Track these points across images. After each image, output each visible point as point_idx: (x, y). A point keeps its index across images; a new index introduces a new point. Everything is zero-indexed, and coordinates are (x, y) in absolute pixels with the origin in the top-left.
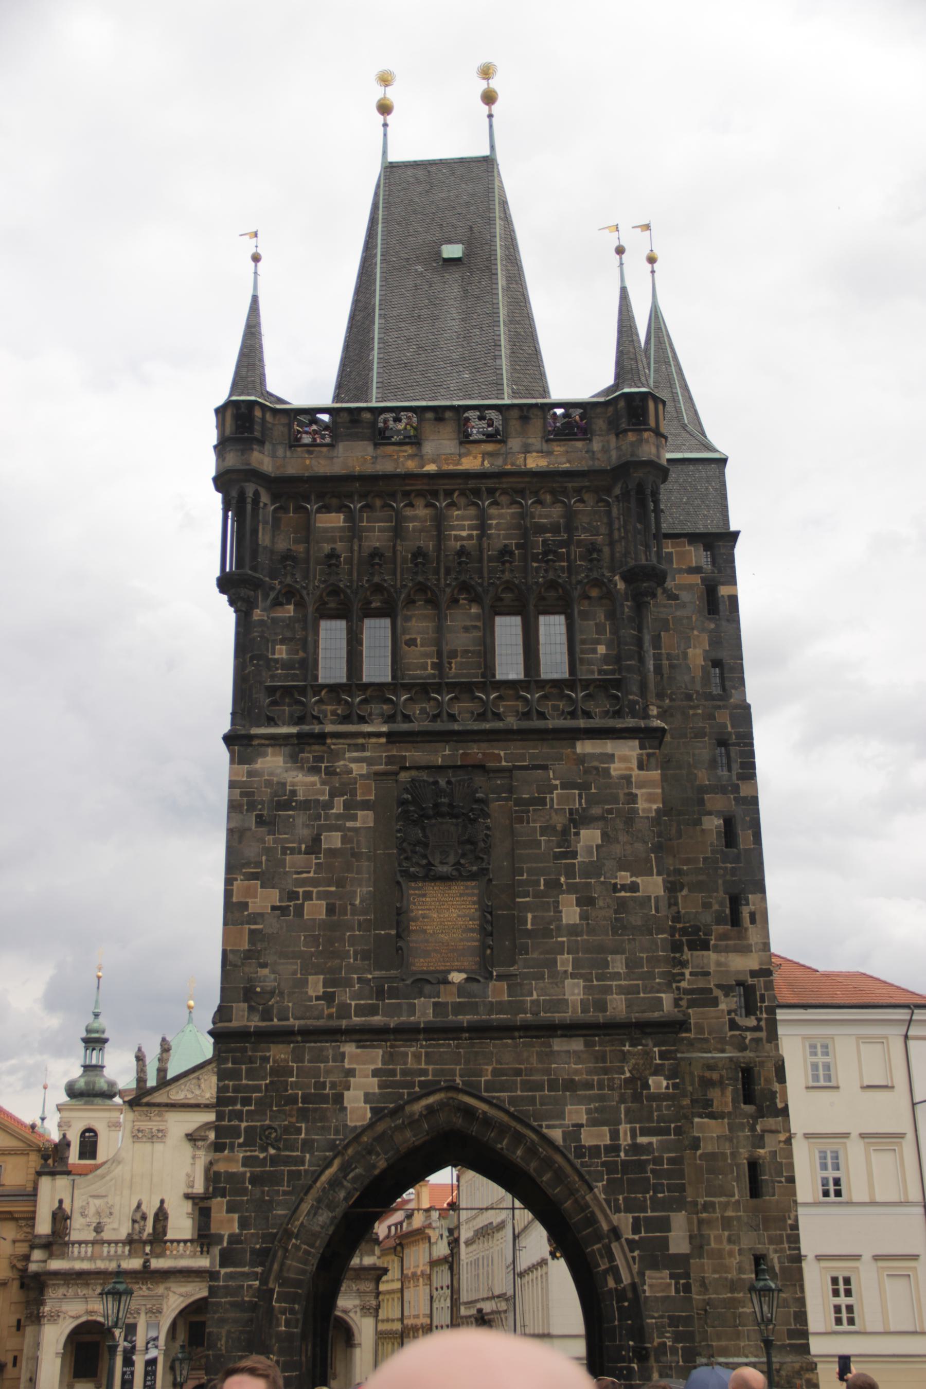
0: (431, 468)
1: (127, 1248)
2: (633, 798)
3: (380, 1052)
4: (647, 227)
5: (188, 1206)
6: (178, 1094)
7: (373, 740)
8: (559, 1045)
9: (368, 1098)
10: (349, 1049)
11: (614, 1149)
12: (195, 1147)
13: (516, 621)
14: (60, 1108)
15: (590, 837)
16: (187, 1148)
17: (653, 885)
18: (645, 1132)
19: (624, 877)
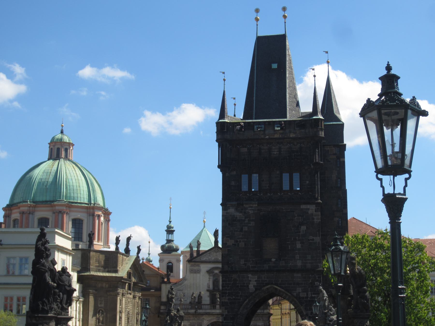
0: (267, 137)
1: (190, 306)
2: (313, 219)
3: (256, 276)
4: (327, 52)
5: (208, 294)
6: (204, 258)
7: (254, 205)
8: (295, 275)
9: (254, 286)
10: (250, 275)
11: (307, 297)
12: (210, 276)
13: (288, 174)
14: (159, 255)
15: (303, 228)
16: (207, 276)
17: (318, 239)
18: (313, 294)
19: (311, 237)
